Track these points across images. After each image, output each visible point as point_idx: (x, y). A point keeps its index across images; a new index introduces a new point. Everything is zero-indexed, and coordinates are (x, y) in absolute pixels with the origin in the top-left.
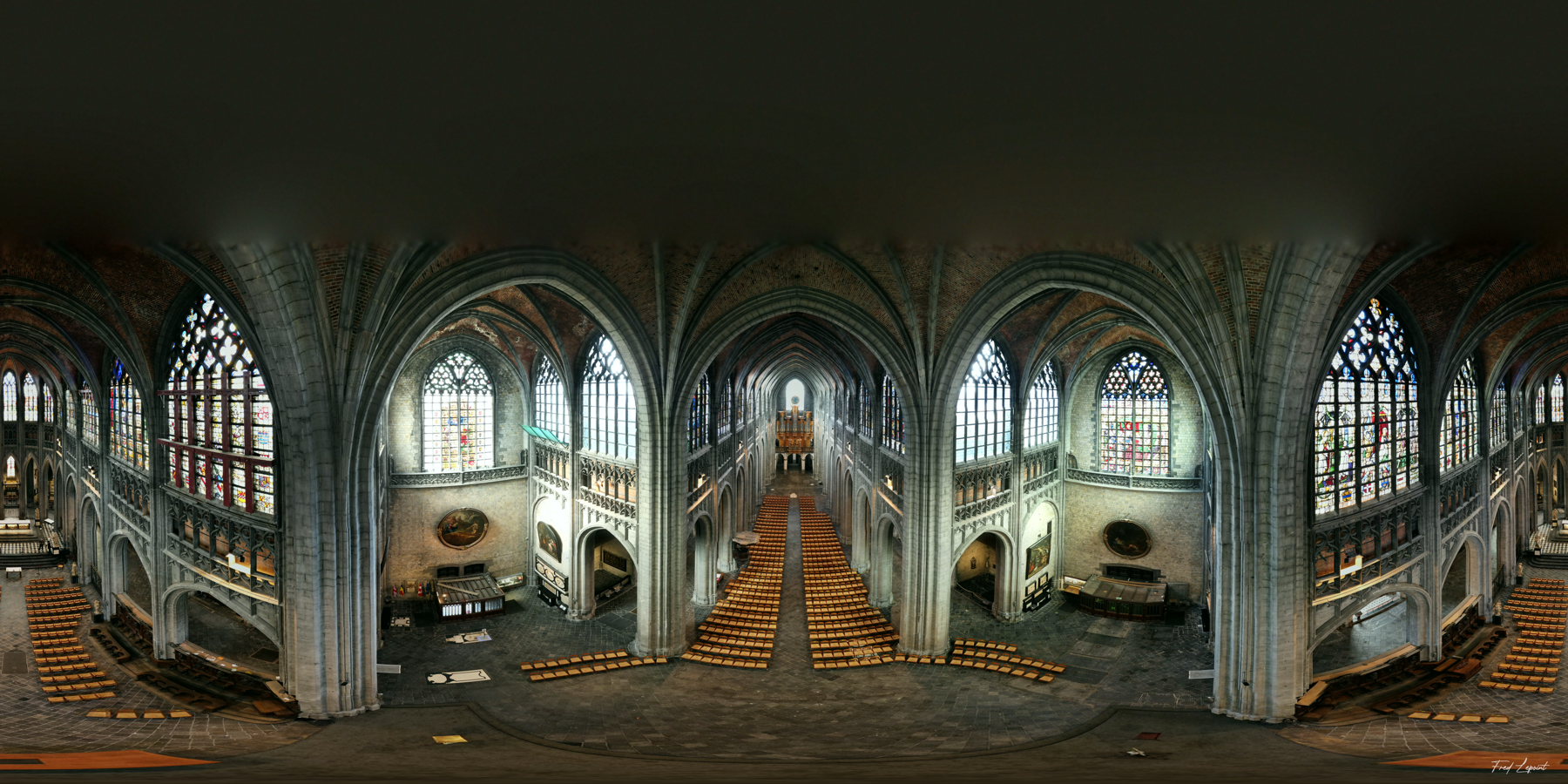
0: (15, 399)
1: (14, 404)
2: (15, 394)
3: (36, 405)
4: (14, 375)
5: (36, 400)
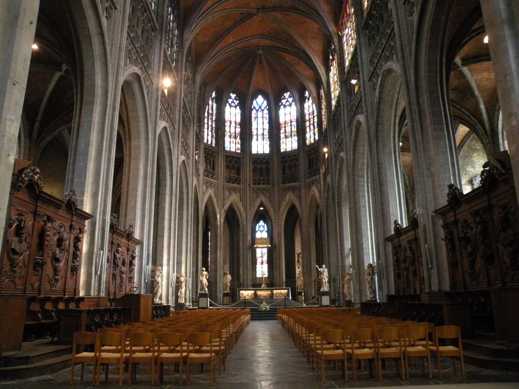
0: (267, 126)
1: (266, 133)
2: (266, 121)
3: (294, 129)
4: (266, 97)
5: (294, 123)
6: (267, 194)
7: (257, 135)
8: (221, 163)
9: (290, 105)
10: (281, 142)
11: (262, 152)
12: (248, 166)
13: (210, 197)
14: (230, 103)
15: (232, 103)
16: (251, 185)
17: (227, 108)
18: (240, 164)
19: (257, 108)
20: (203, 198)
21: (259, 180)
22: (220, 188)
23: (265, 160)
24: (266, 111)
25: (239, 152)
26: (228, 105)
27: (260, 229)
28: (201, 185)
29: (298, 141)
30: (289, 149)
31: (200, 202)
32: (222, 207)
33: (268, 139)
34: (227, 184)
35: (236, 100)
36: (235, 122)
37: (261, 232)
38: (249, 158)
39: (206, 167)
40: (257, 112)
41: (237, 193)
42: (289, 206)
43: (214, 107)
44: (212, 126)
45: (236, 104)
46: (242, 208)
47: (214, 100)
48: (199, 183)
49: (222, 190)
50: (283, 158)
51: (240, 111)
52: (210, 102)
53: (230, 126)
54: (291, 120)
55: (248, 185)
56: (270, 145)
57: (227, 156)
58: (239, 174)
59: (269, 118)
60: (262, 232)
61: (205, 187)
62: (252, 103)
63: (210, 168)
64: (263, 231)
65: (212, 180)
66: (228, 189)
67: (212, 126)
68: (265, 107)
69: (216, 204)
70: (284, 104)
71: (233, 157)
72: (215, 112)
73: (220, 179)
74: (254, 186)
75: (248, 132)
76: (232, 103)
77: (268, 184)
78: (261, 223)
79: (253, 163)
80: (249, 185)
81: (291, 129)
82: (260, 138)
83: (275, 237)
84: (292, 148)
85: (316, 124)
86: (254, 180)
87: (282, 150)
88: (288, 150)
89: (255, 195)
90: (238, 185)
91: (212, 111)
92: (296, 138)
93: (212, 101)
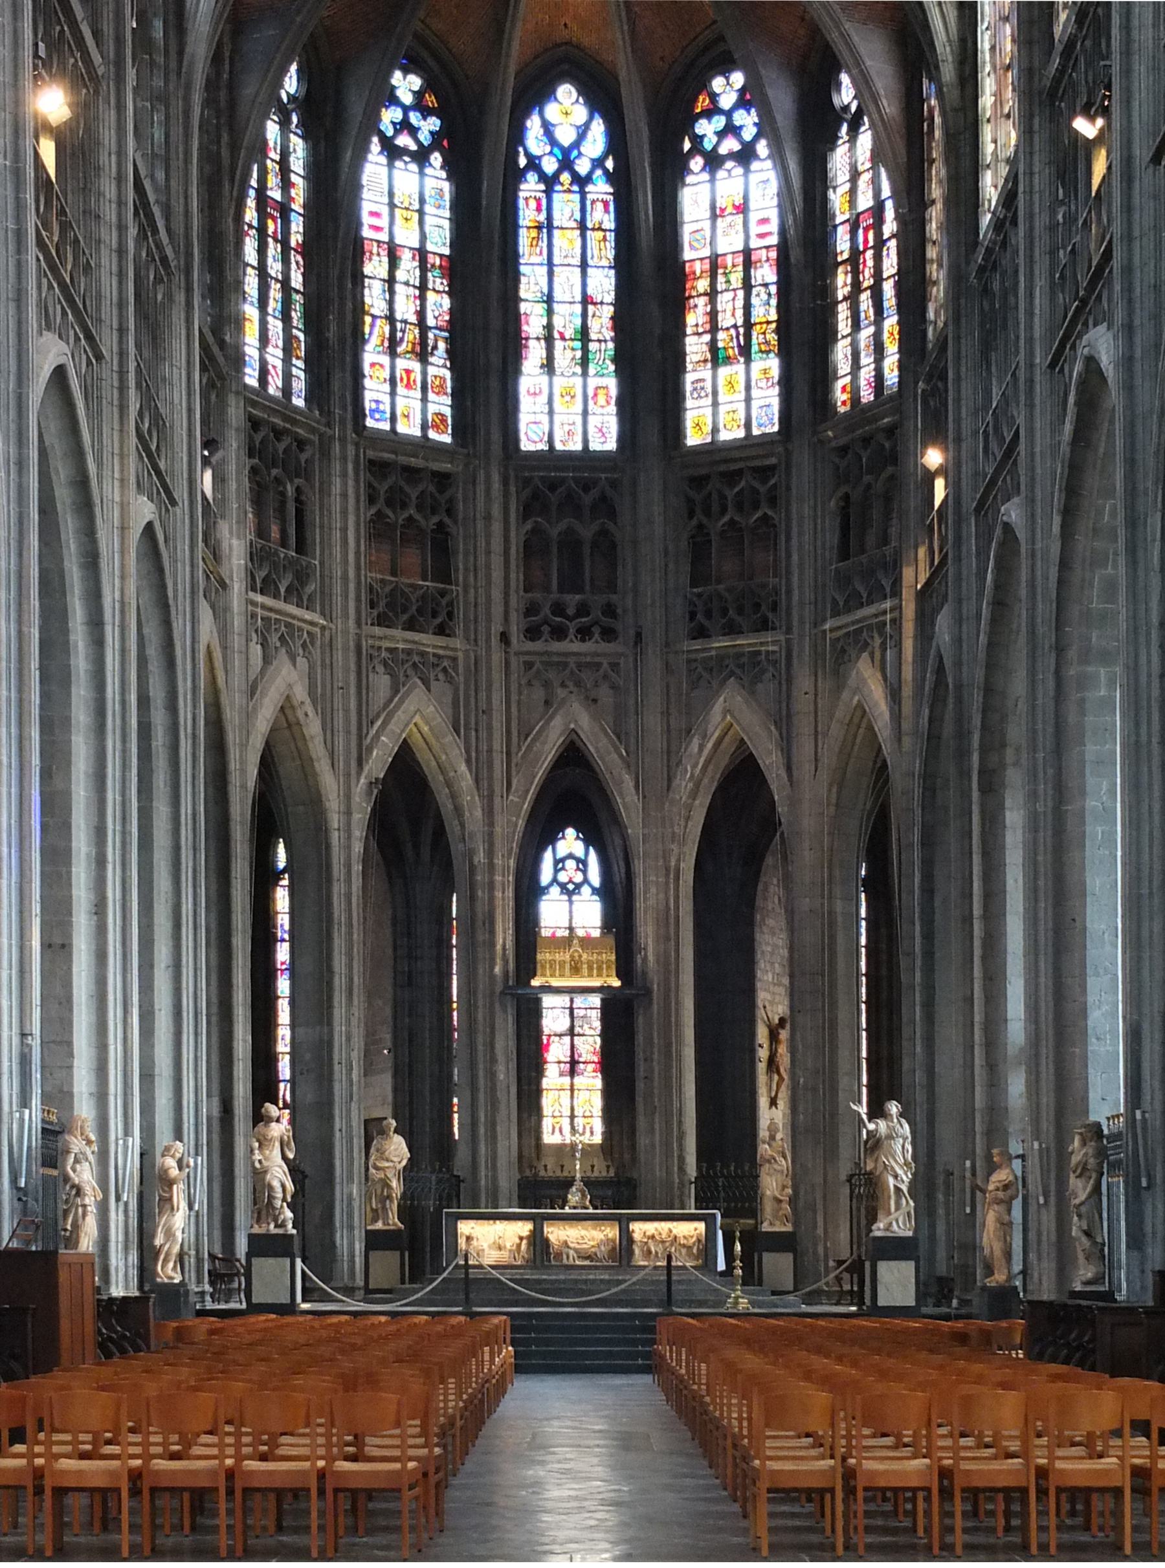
0: (603, 284)
1: (601, 323)
2: (603, 251)
5: (766, 274)
6: (605, 695)
7: (549, 340)
8: (344, 512)
9: (745, 156)
10: (688, 387)
11: (576, 446)
12: (497, 527)
13: (286, 708)
14: (390, 132)
15: (397, 132)
16: (514, 640)
17: (374, 166)
18: (450, 512)
19: (550, 166)
20: (249, 716)
21: (559, 609)
22: (339, 656)
23: (594, 493)
24: (600, 188)
25: (447, 439)
26: (375, 145)
27: (563, 877)
28: (237, 642)
29: (786, 383)
30: (731, 433)
31: (232, 737)
32: (354, 764)
33: (612, 368)
34: (378, 631)
35: (426, 112)
36: (422, 254)
37: (570, 891)
38: (505, 482)
39: (261, 532)
40: (549, 192)
41: (434, 684)
42: (724, 761)
43: (297, 164)
44: (285, 283)
45: (425, 137)
46: (463, 767)
47: (295, 119)
48: (223, 631)
49: (353, 666)
50: (698, 482)
51: (446, 186)
52: (272, 130)
53: (391, 281)
54: (747, 253)
55: (495, 641)
56: (621, 403)
57: (378, 468)
58: (444, 573)
59: (618, 231)
60: (570, 894)
61: (256, 650)
62: (517, 135)
63: (284, 543)
64: (578, 886)
65: (292, 609)
66: (385, 663)
67: (285, 283)
68: (598, 163)
69: (317, 749)
70: (708, 145)
71: (411, 473)
72: (299, 194)
73: (338, 600)
74: (530, 646)
75: (496, 322)
76: (397, 132)
77: (609, 634)
78: (570, 842)
79: (526, 512)
80: (504, 638)
81: (747, 307)
82: (565, 356)
83: (646, 932)
84: (748, 425)
85: (888, 288)
86: (531, 610)
87: (693, 438)
88: (724, 436)
89: (539, 694)
90: (440, 641)
91: (286, 185)
92: (773, 364)
93: (284, 124)
